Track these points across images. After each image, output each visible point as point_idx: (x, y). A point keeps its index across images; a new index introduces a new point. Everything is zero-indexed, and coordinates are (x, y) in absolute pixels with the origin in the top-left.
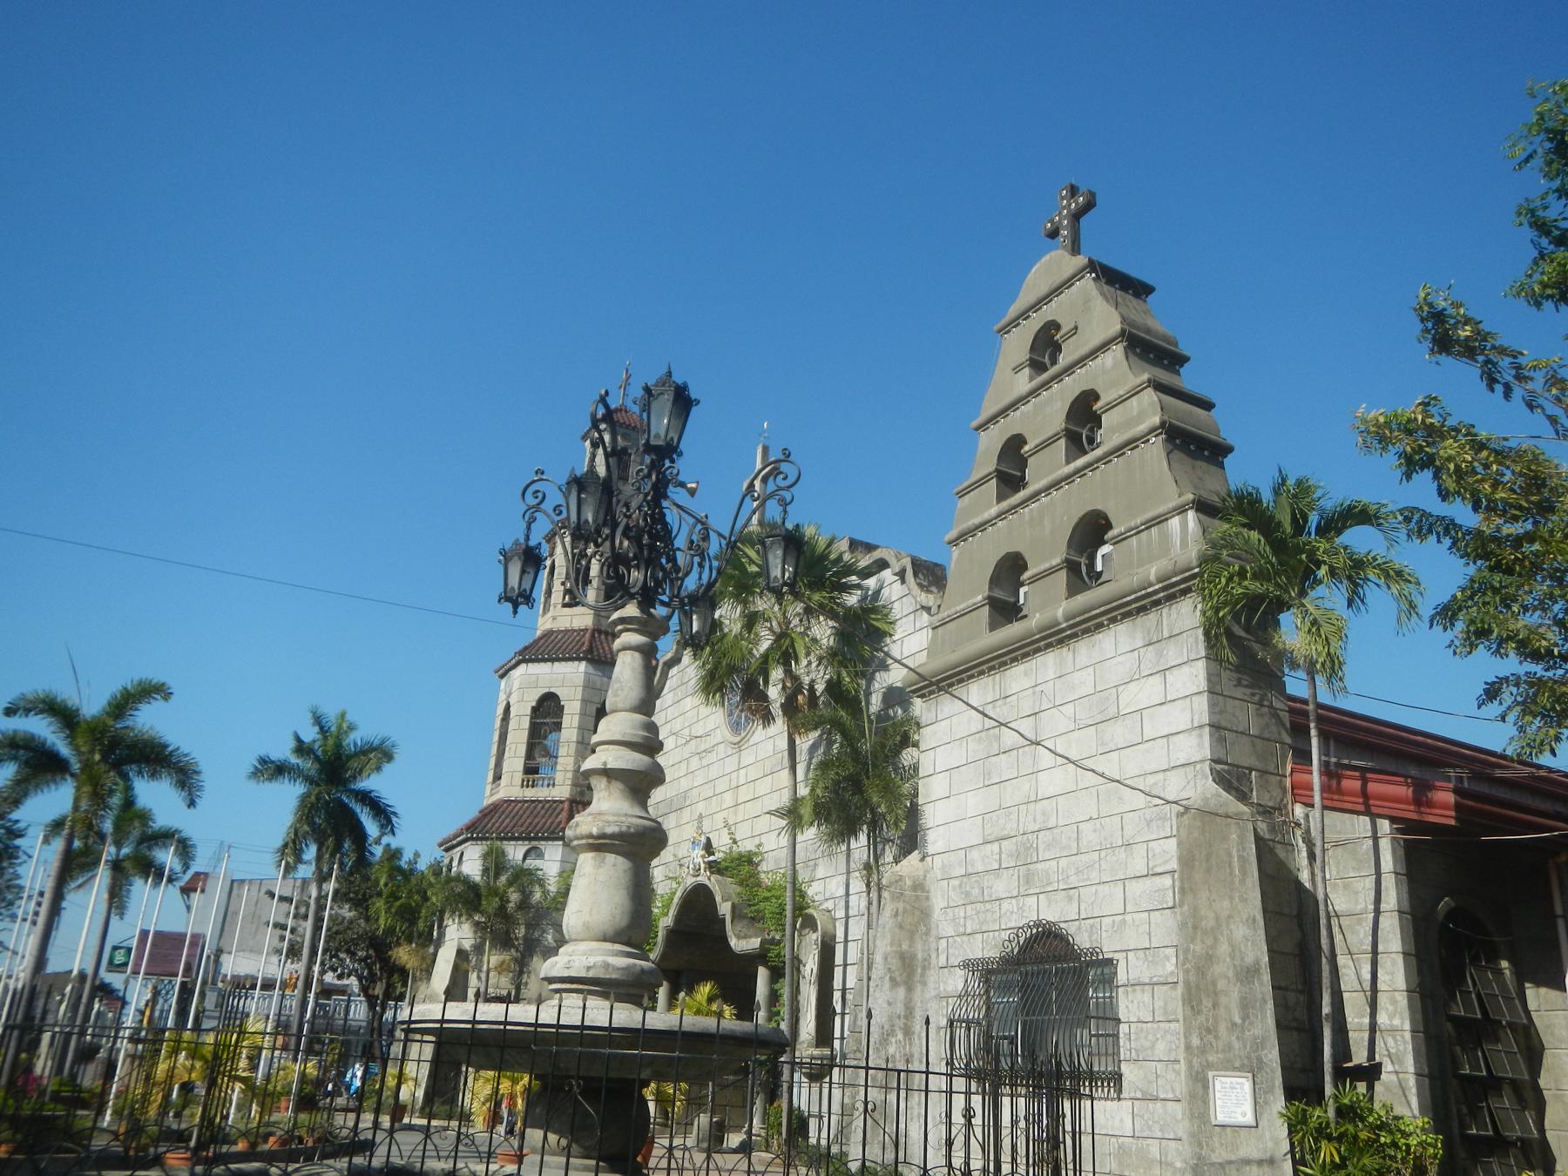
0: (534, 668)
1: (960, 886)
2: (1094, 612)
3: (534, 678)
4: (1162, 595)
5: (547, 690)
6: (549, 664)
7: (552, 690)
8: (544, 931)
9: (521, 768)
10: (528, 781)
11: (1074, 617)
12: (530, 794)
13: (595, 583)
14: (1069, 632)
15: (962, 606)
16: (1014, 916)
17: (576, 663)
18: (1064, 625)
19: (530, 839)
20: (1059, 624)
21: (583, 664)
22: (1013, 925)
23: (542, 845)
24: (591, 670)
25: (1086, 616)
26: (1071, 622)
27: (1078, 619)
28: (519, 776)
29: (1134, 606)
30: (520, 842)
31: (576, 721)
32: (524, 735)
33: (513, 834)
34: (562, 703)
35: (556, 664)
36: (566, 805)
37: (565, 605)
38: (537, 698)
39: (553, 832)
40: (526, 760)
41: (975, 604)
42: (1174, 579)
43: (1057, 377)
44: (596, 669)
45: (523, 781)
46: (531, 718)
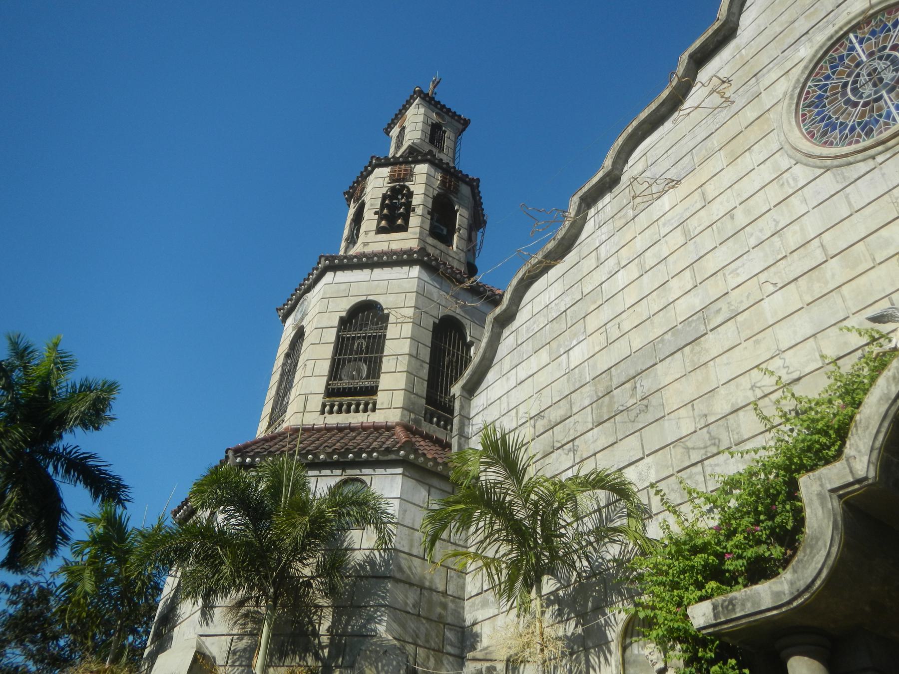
0: (342, 276)
3: (343, 286)
5: (364, 298)
6: (367, 272)
7: (370, 298)
8: (371, 619)
9: (322, 390)
10: (332, 406)
12: (334, 420)
13: (419, 211)
17: (406, 268)
19: (343, 465)
21: (416, 271)
23: (366, 474)
24: (425, 277)
28: (316, 402)
30: (328, 472)
31: (408, 329)
32: (328, 351)
33: (316, 456)
34: (386, 311)
35: (377, 271)
36: (398, 429)
37: (380, 230)
38: (348, 307)
39: (388, 451)
40: (330, 379)
44: (433, 280)
45: (324, 406)
46: (338, 331)
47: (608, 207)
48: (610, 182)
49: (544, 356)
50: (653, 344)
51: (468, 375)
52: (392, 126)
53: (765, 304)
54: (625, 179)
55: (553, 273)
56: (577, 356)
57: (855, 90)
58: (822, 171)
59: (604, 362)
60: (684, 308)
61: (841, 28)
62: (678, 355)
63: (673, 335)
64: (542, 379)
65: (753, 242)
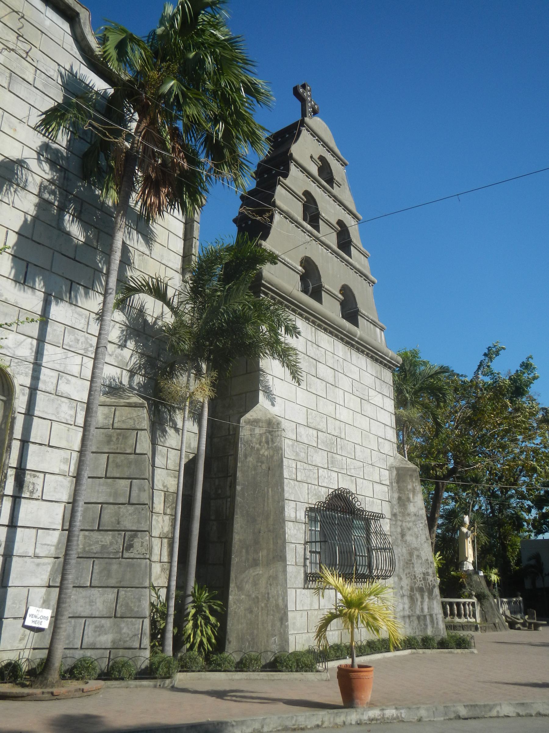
1: (293, 446)
2: (368, 346)
4: (386, 362)
11: (367, 344)
14: (354, 343)
15: (289, 260)
16: (326, 480)
18: (356, 339)
20: (355, 336)
22: (325, 485)
25: (365, 344)
26: (359, 341)
27: (362, 342)
29: (377, 357)
41: (296, 268)
42: (393, 361)
43: (336, 199)
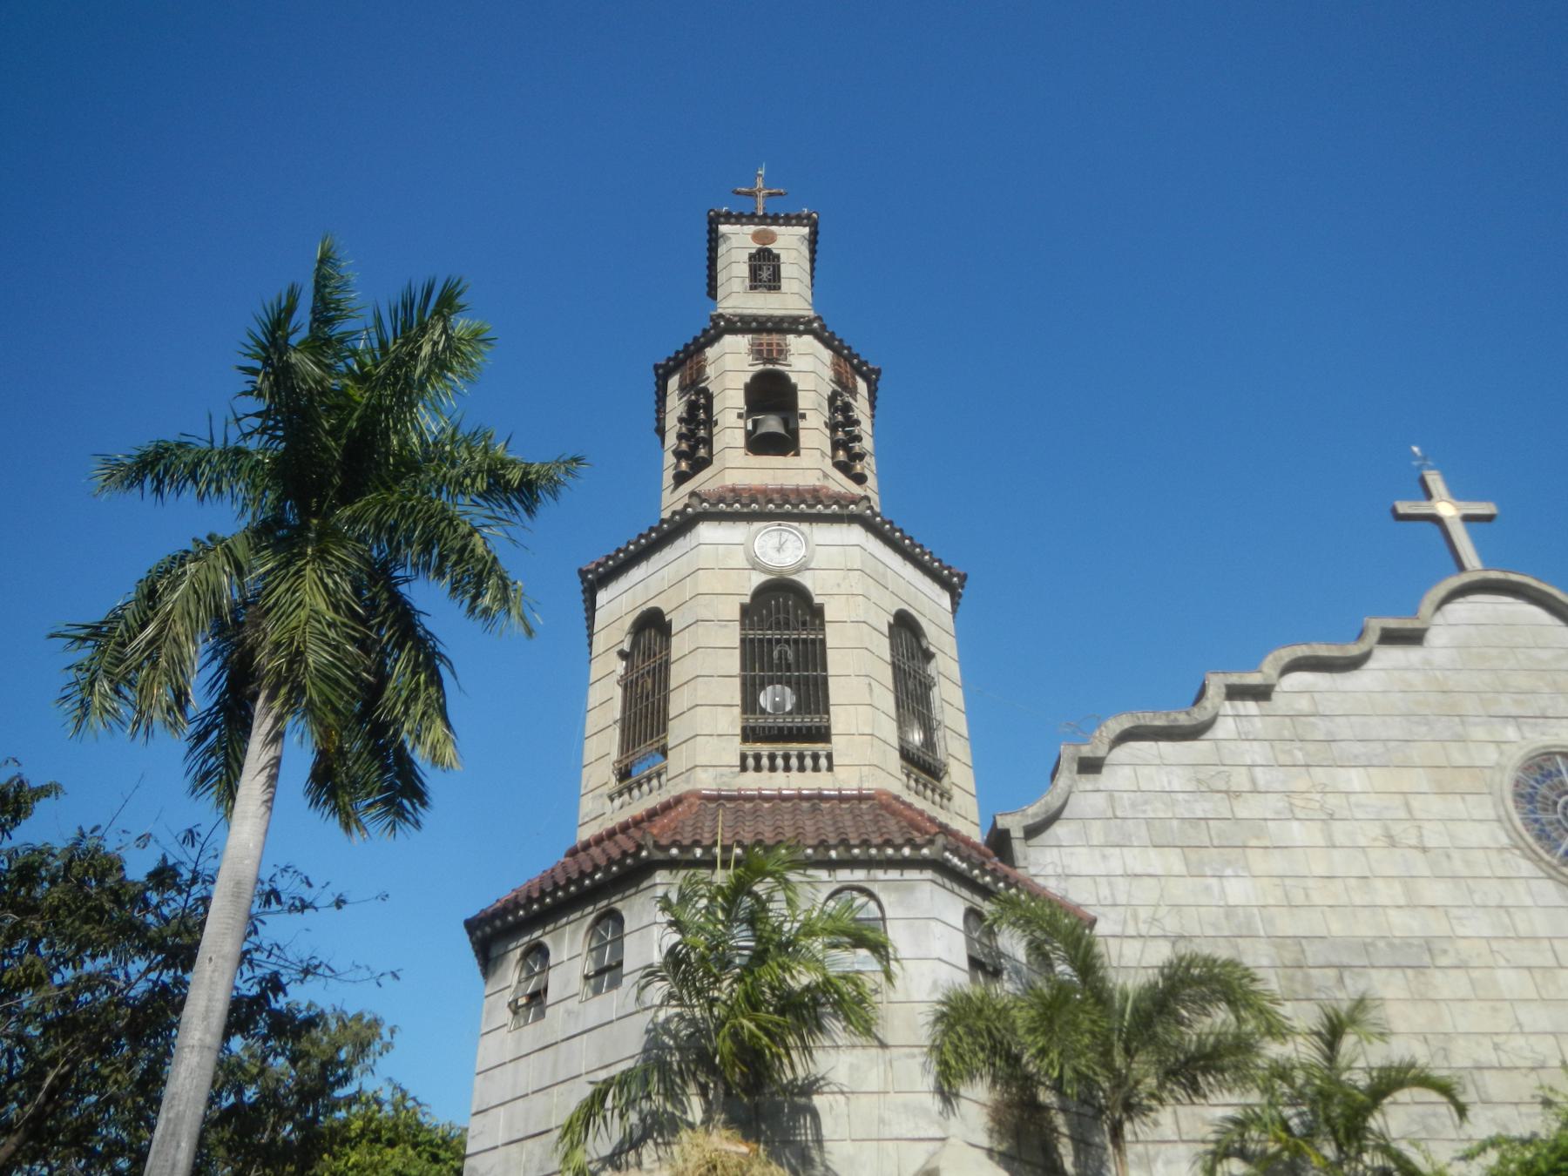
38: (894, 612)
47: (1258, 722)
48: (1261, 693)
49: (1174, 861)
50: (1366, 946)
51: (1036, 815)
52: (733, 220)
53: (1499, 973)
54: (1279, 701)
55: (1165, 747)
56: (1238, 891)
57: (1565, 814)
58: (1541, 874)
59: (1287, 925)
60: (1404, 924)
61: (1555, 746)
62: (1398, 973)
63: (1391, 945)
64: (1180, 891)
65: (1478, 899)
